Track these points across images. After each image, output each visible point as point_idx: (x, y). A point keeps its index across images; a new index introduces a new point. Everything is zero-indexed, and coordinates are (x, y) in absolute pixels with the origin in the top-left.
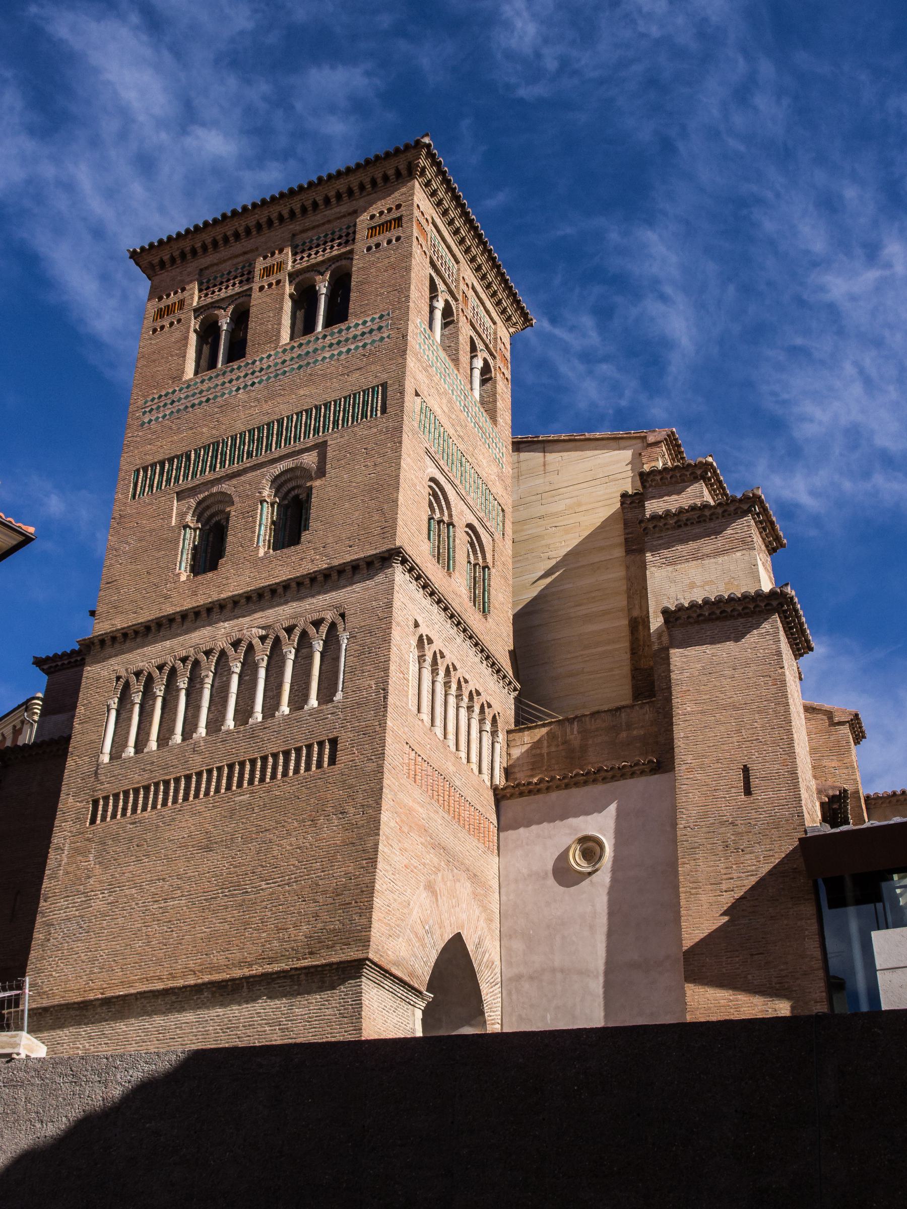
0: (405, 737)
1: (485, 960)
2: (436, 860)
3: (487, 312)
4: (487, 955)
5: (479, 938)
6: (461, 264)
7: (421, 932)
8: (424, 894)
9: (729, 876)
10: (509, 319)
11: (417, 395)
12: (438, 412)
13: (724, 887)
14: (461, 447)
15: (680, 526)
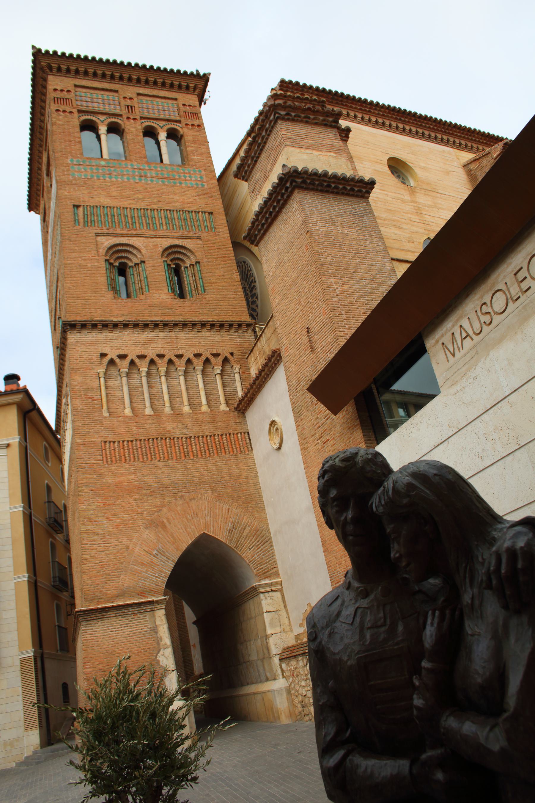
0: (101, 439)
1: (245, 534)
2: (157, 502)
3: (165, 98)
4: (248, 529)
5: (233, 524)
6: (120, 91)
7: (147, 559)
8: (147, 532)
9: (318, 425)
10: (188, 87)
11: (78, 207)
12: (106, 201)
13: (317, 436)
14: (143, 205)
15: (256, 161)
